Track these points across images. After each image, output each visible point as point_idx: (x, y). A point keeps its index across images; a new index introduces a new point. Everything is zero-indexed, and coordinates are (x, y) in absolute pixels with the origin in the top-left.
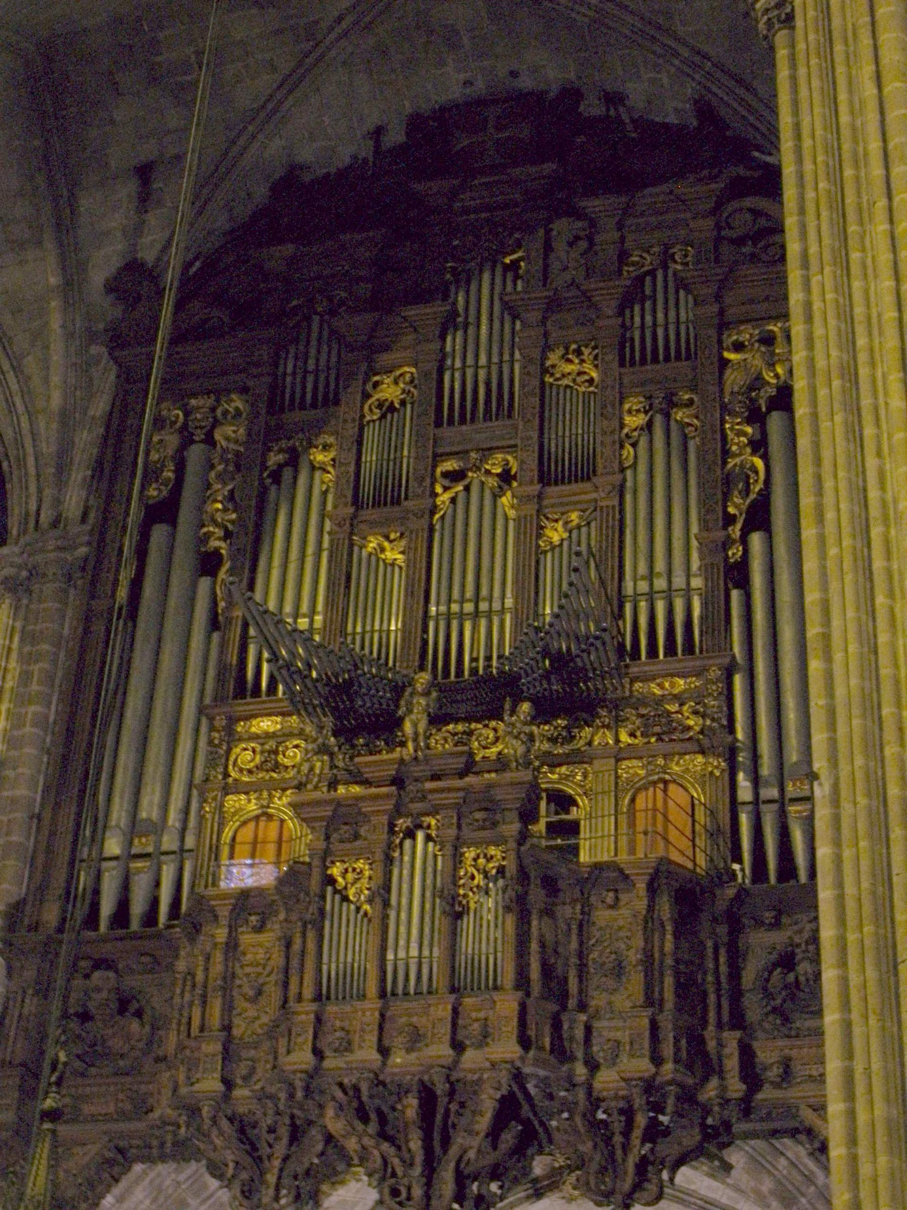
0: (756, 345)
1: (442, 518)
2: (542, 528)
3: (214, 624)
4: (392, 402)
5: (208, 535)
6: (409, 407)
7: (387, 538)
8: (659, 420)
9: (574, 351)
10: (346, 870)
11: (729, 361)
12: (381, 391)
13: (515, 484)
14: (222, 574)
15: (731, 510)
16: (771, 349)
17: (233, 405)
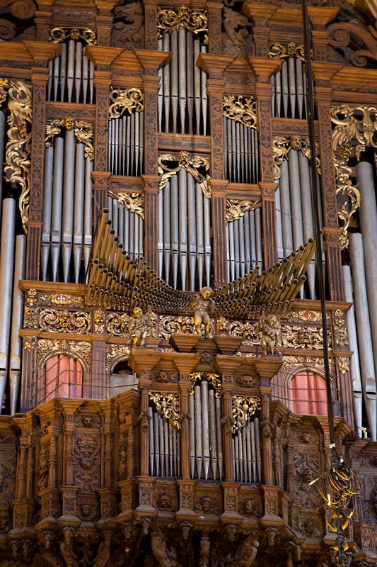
0: (352, 118)
1: (163, 189)
2: (228, 207)
3: (18, 229)
4: (127, 109)
5: (11, 171)
6: (137, 114)
7: (131, 196)
8: (294, 153)
9: (241, 100)
10: (162, 399)
11: (336, 125)
12: (119, 101)
13: (208, 177)
14: (22, 199)
15: (342, 217)
16: (361, 122)
17: (20, 89)
